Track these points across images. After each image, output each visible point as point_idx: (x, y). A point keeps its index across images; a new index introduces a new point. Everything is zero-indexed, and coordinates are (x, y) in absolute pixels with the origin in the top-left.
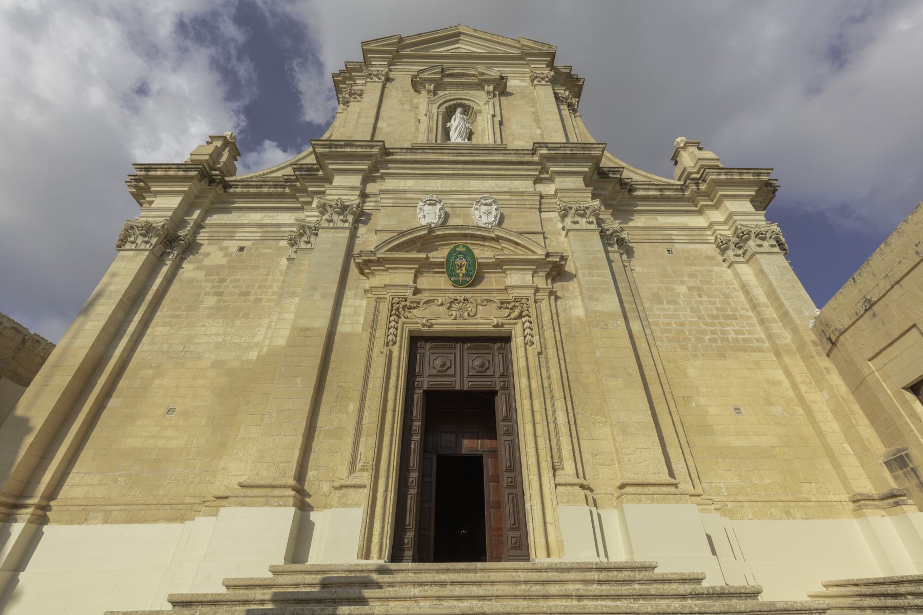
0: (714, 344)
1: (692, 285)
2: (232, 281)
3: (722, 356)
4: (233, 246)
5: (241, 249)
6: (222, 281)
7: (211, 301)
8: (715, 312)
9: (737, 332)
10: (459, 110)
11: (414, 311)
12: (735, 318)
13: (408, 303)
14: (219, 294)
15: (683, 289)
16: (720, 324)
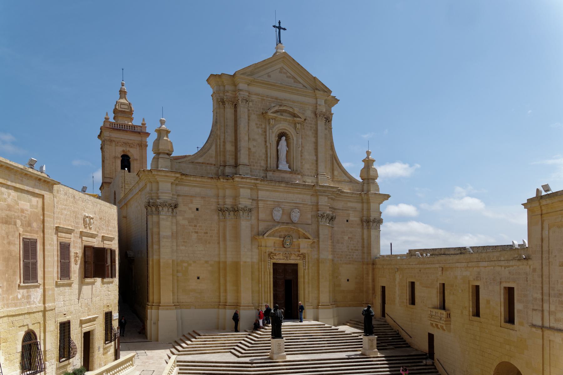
0: (349, 259)
1: (349, 236)
2: (200, 226)
3: (350, 263)
4: (194, 206)
5: (197, 209)
6: (195, 226)
7: (194, 236)
8: (353, 248)
9: (357, 255)
10: (284, 138)
11: (275, 257)
12: (357, 250)
13: (273, 255)
14: (197, 232)
15: (346, 238)
16: (353, 252)
